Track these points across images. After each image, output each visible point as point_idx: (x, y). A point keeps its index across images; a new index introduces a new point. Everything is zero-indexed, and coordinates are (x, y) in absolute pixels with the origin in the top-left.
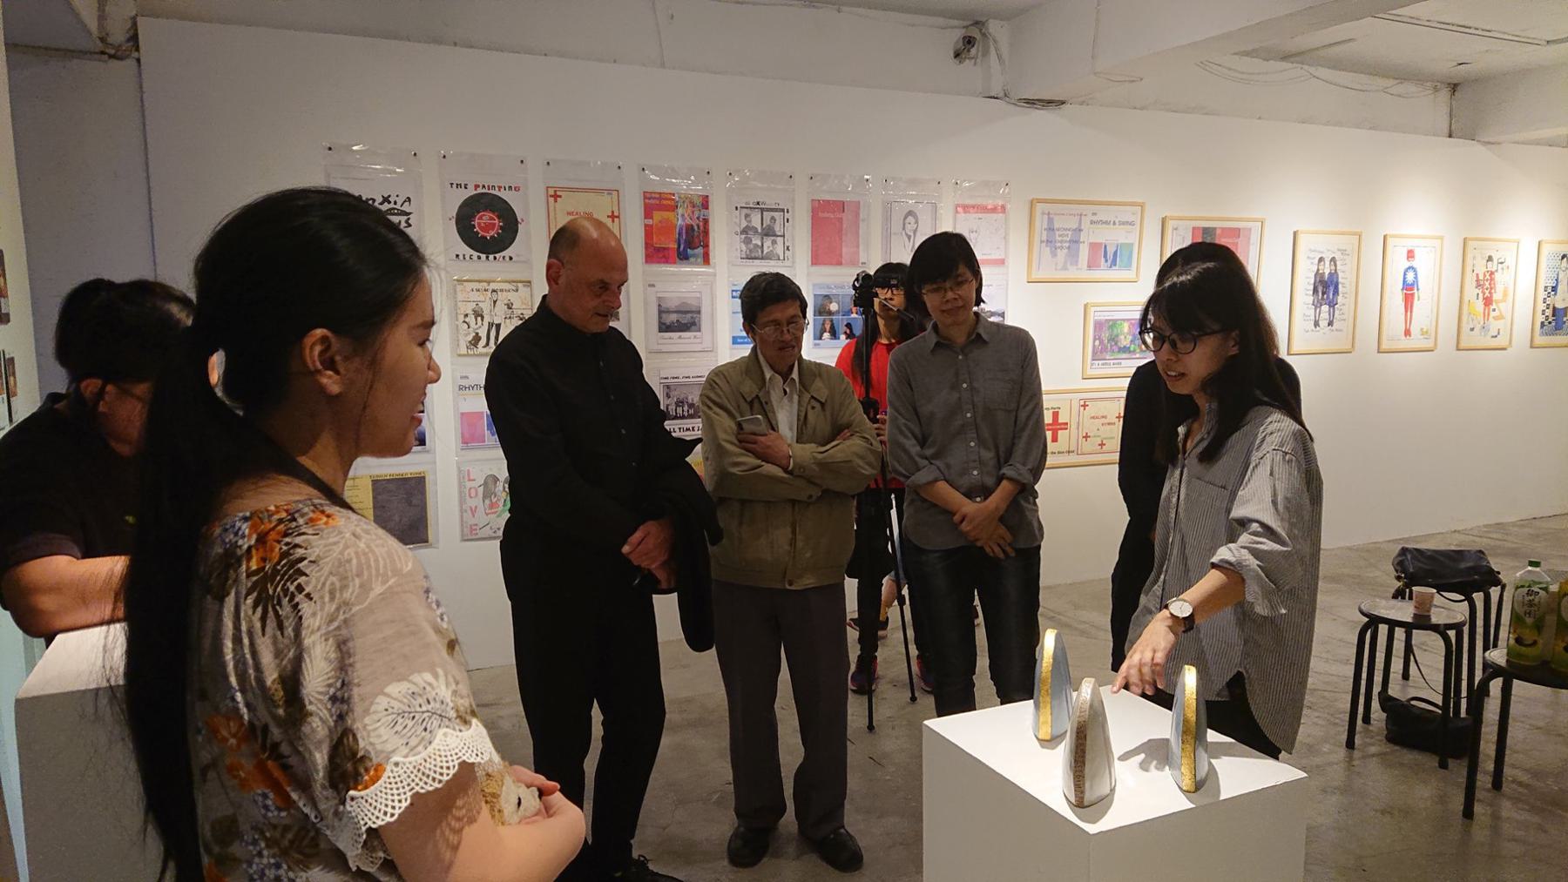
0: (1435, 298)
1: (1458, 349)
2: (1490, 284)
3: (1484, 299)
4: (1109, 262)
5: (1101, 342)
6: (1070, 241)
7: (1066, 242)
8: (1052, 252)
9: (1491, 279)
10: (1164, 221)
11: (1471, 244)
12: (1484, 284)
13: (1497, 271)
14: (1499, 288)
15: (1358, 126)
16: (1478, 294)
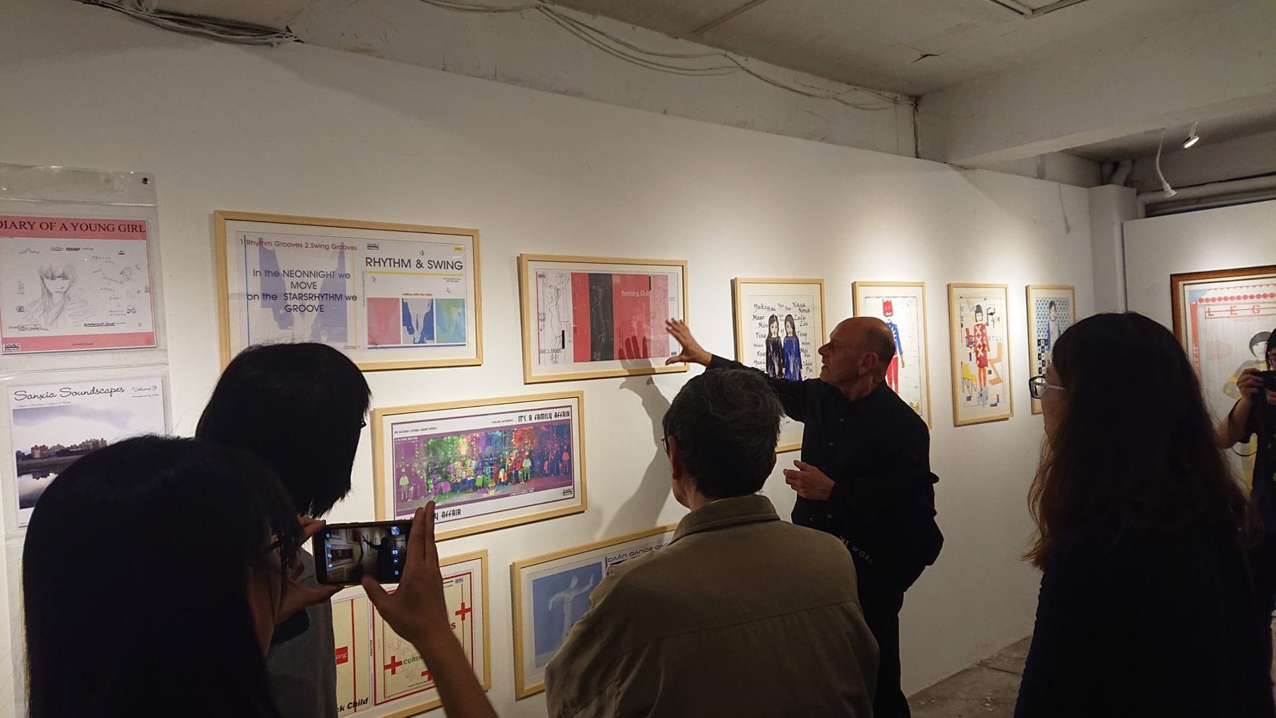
0: (923, 356)
1: (956, 426)
2: (982, 340)
3: (978, 359)
4: (417, 335)
5: (413, 478)
6: (321, 296)
7: (311, 297)
8: (278, 318)
9: (984, 335)
10: (519, 260)
11: (956, 292)
12: (976, 341)
13: (987, 324)
14: (992, 345)
15: (810, 137)
16: (970, 354)
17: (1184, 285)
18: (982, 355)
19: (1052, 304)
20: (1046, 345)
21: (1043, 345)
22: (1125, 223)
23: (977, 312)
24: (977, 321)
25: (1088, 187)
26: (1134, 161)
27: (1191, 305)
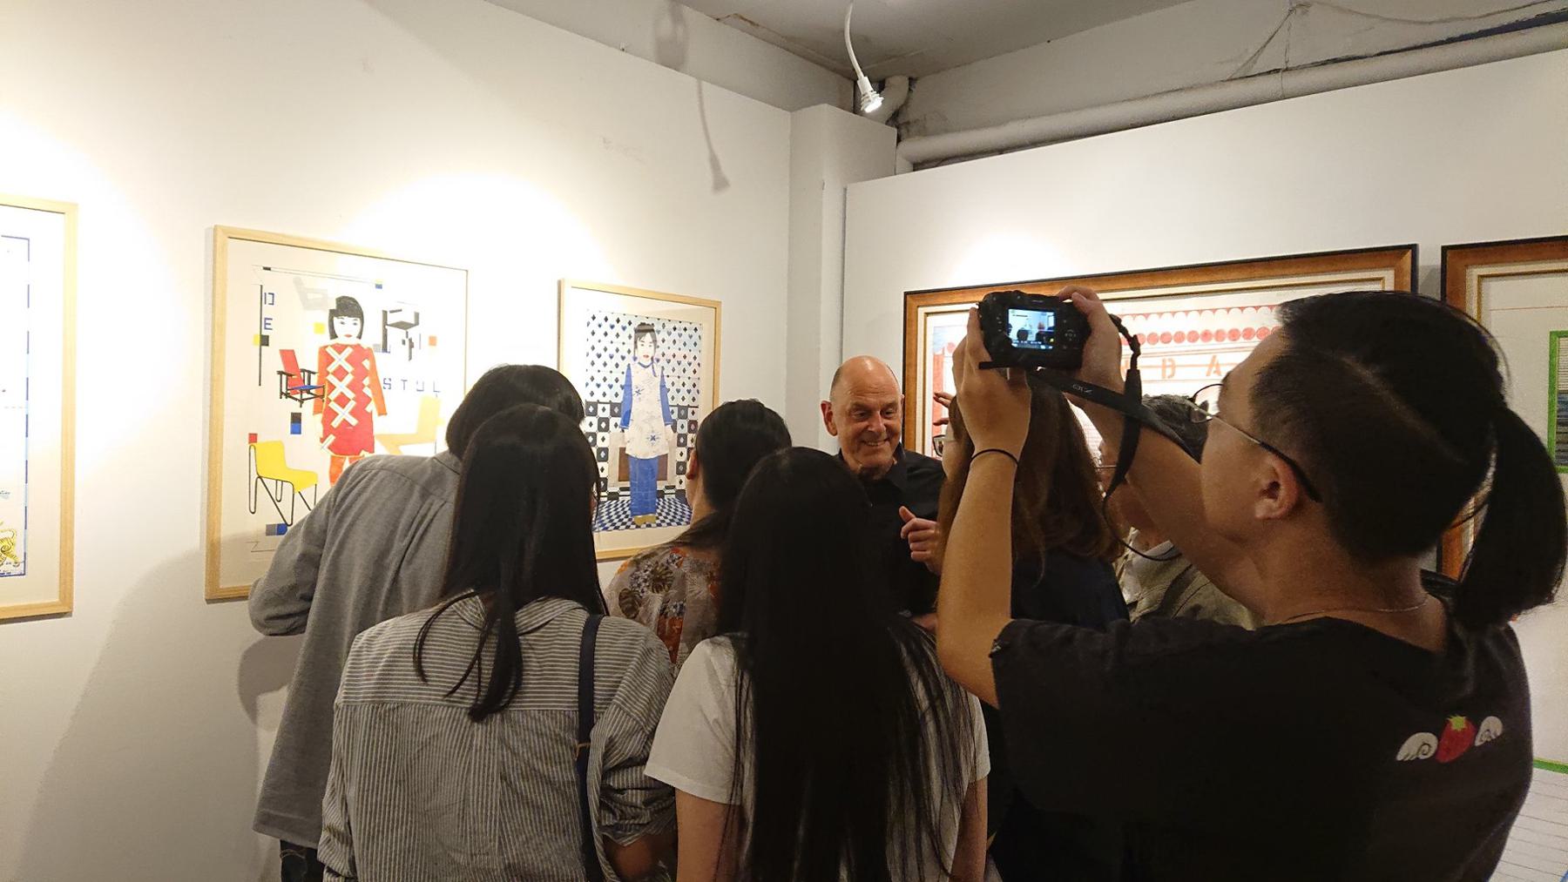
2: (355, 386)
3: (328, 430)
9: (361, 373)
13: (385, 349)
16: (296, 419)
17: (927, 314)
18: (353, 421)
19: (644, 329)
20: (613, 414)
21: (607, 414)
22: (851, 187)
23: (333, 313)
24: (334, 335)
25: (791, 111)
26: (912, 81)
27: (935, 356)
